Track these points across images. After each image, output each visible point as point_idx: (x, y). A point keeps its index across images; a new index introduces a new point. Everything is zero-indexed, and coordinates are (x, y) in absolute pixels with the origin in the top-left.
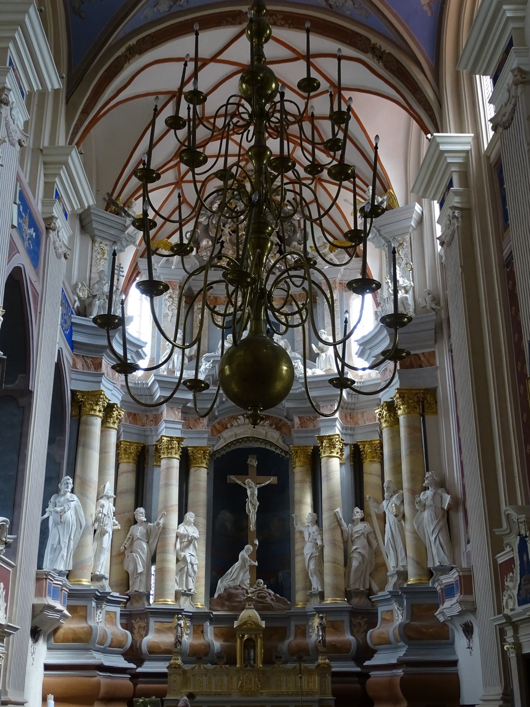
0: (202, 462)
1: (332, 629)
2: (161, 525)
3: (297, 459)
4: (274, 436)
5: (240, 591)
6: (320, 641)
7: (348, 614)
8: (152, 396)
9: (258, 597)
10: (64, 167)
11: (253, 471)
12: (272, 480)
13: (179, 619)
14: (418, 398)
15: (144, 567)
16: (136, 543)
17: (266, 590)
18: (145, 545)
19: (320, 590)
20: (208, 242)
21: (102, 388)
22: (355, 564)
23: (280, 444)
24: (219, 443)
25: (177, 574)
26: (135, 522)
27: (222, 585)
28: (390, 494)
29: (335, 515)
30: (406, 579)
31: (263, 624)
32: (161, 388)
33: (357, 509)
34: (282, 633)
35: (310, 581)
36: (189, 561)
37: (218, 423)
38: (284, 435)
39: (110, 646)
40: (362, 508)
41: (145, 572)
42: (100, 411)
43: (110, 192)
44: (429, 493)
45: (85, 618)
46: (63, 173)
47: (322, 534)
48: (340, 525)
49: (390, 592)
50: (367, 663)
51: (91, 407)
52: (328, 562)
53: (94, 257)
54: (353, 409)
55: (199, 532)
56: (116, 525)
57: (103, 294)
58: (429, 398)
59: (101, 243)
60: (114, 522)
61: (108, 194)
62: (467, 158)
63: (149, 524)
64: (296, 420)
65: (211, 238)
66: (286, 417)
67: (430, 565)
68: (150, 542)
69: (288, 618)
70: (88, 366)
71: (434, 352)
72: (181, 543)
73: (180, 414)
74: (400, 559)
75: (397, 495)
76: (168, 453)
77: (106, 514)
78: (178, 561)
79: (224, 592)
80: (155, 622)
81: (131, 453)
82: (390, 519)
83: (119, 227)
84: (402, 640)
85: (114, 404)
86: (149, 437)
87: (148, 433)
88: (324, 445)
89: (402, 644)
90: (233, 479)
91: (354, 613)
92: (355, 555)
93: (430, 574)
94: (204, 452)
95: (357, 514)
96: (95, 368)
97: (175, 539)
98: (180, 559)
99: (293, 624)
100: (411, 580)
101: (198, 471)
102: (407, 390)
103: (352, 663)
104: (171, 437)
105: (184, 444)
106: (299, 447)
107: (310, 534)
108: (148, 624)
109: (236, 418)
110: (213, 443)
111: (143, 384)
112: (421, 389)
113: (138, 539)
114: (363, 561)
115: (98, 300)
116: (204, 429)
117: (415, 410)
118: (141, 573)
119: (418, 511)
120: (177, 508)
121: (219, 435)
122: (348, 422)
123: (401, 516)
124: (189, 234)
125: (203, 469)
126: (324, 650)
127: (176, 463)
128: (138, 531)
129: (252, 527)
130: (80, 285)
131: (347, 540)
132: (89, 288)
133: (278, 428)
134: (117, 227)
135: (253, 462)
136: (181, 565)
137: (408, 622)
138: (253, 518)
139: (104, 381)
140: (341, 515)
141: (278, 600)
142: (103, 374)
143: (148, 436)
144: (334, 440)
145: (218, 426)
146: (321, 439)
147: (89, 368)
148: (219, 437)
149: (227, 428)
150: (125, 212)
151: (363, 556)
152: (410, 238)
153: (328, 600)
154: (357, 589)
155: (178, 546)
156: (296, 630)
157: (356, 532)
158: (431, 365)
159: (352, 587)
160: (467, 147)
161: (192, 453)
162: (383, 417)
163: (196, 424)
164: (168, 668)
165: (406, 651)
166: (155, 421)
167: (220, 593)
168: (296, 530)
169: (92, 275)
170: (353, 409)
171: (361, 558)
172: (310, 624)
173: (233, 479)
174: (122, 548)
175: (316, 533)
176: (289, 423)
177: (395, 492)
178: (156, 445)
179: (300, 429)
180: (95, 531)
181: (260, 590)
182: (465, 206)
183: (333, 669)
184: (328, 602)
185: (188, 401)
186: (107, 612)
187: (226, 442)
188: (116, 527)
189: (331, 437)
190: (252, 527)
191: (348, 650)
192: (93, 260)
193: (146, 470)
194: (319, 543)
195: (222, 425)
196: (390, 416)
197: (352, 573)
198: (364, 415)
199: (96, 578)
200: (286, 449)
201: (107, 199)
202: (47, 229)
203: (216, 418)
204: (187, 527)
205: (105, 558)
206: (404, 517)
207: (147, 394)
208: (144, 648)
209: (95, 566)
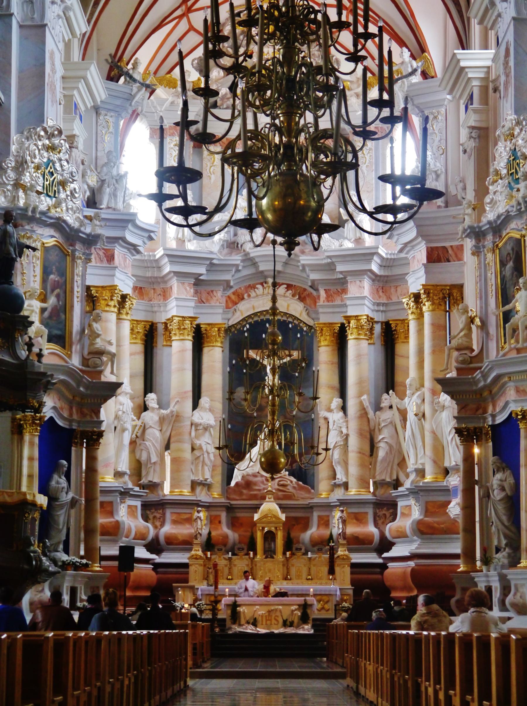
0: (216, 341)
1: (355, 521)
2: (175, 413)
3: (322, 338)
5: (259, 479)
6: (340, 534)
7: (372, 506)
8: (159, 268)
9: (278, 485)
10: (82, 81)
13: (198, 512)
14: (443, 294)
15: (157, 456)
16: (148, 432)
17: (287, 477)
18: (158, 433)
19: (344, 480)
20: (219, 72)
21: (117, 282)
22: (381, 453)
23: (304, 317)
24: (235, 317)
25: (192, 463)
26: (145, 408)
28: (412, 392)
29: (361, 403)
30: (423, 476)
31: (283, 517)
32: (171, 262)
34: (305, 524)
35: (334, 471)
36: (205, 450)
37: (234, 293)
38: (309, 308)
39: (134, 539)
41: (159, 462)
42: (115, 306)
43: (113, 53)
45: (111, 513)
46: (82, 86)
47: (347, 422)
48: (366, 413)
49: (407, 489)
50: (385, 555)
51: (106, 303)
52: (353, 451)
53: (99, 132)
54: (386, 282)
55: (215, 418)
56: (134, 421)
57: (112, 178)
58: (455, 293)
59: (106, 115)
60: (132, 418)
61: (110, 55)
62: (488, 73)
63: (163, 411)
64: (322, 293)
66: (311, 287)
67: (447, 464)
68: (163, 431)
69: (310, 508)
70: (100, 258)
71: (462, 245)
72: (196, 430)
73: (192, 290)
74: (419, 457)
75: (419, 393)
76: (181, 334)
77: (124, 410)
78: (193, 449)
79: (242, 479)
80: (172, 513)
81: (138, 332)
82: (411, 417)
83: (126, 96)
84: (414, 534)
85: (127, 295)
86: (157, 313)
87: (155, 309)
88: (351, 325)
89: (415, 538)
92: (382, 445)
93: (446, 472)
94: (219, 330)
95: (386, 401)
96: (108, 261)
97: (189, 427)
98: (195, 447)
99: (316, 515)
100: (428, 478)
101: (211, 352)
102: (433, 286)
103: (374, 555)
104: (183, 317)
105: (198, 321)
106: (325, 324)
107: (334, 422)
108: (164, 514)
109: (253, 287)
110: (229, 316)
111: (150, 256)
112: (446, 286)
113: (151, 427)
114: (391, 450)
115: (108, 187)
116: (218, 304)
117: (440, 307)
118: (154, 463)
119: (437, 411)
120: (190, 394)
121: (235, 307)
122: (380, 297)
123: (421, 415)
124: (196, 61)
125: (217, 348)
126: (345, 542)
127: (189, 345)
128: (150, 417)
130: (89, 172)
131: (374, 429)
132: (96, 169)
133: (302, 299)
134: (121, 96)
136: (197, 453)
137: (421, 517)
139: (118, 274)
140: (366, 404)
141: (301, 488)
142: (116, 267)
143: (156, 312)
144: (362, 321)
145: (233, 297)
146: (348, 318)
147: (102, 261)
148: (235, 310)
149: (243, 299)
150: (131, 77)
151: (391, 446)
152: (446, 110)
154: (384, 480)
155: (193, 434)
156: (319, 521)
157: (383, 421)
158: (459, 260)
160: (489, 63)
161: (206, 330)
162: (410, 308)
163: (209, 298)
164: (189, 559)
165: (419, 545)
166: (164, 296)
167: (237, 480)
168: (320, 416)
169: (99, 154)
170: (386, 282)
171: (388, 448)
172: (333, 514)
174: (134, 436)
175: (341, 421)
176: (314, 293)
177: (417, 390)
178: (166, 324)
179: (326, 303)
180: (115, 428)
181: (280, 477)
182: (483, 125)
183: (353, 561)
184: (352, 493)
185: (201, 275)
186: (129, 507)
187: (242, 315)
188: (134, 423)
189: (359, 318)
191: (371, 542)
192: (99, 136)
193: (155, 350)
194: (345, 431)
195: (238, 296)
196: (417, 308)
197: (378, 464)
198: (399, 289)
199: (118, 474)
200: (311, 323)
201: (110, 60)
202: (70, 147)
203: (231, 287)
204: (202, 413)
205: (125, 455)
206: (424, 415)
207: (154, 265)
208: (162, 539)
209: (117, 463)
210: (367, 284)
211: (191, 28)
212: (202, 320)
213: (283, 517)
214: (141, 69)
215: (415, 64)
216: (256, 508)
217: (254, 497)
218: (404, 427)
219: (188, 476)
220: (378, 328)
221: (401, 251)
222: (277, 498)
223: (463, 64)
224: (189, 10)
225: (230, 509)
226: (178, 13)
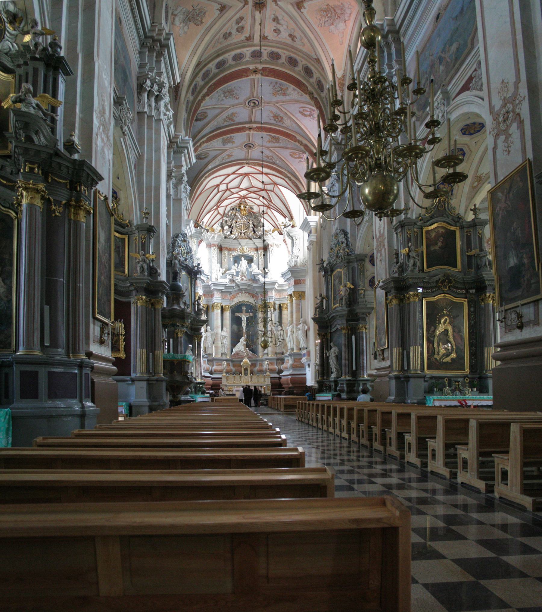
4: (251, 300)
8: (210, 288)
11: (244, 312)
12: (251, 314)
27: (235, 350)
31: (250, 363)
33: (279, 327)
40: (281, 326)
44: (301, 325)
65: (228, 225)
69: (257, 361)
90: (237, 314)
91: (278, 359)
99: (258, 363)
109: (238, 294)
127: (219, 311)
129: (244, 331)
133: (253, 297)
135: (244, 308)
138: (244, 328)
153: (270, 356)
159: (277, 351)
173: (237, 314)
190: (244, 331)
210: (274, 292)
211: (219, 213)
212: (224, 304)
213: (250, 363)
214: (204, 224)
215: (290, 223)
216: (241, 361)
217: (239, 358)
218: (287, 337)
219: (220, 351)
220: (277, 306)
221: (285, 281)
222: (248, 358)
223: (308, 220)
224: (218, 207)
225: (232, 361)
226: (215, 207)
